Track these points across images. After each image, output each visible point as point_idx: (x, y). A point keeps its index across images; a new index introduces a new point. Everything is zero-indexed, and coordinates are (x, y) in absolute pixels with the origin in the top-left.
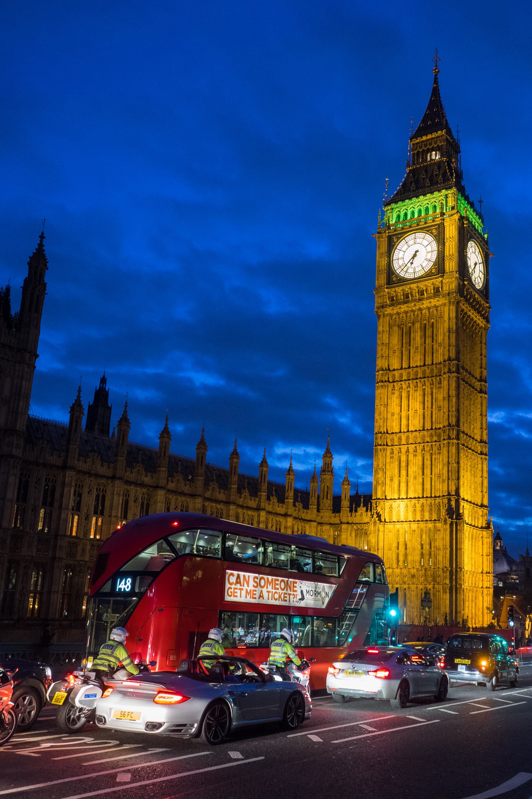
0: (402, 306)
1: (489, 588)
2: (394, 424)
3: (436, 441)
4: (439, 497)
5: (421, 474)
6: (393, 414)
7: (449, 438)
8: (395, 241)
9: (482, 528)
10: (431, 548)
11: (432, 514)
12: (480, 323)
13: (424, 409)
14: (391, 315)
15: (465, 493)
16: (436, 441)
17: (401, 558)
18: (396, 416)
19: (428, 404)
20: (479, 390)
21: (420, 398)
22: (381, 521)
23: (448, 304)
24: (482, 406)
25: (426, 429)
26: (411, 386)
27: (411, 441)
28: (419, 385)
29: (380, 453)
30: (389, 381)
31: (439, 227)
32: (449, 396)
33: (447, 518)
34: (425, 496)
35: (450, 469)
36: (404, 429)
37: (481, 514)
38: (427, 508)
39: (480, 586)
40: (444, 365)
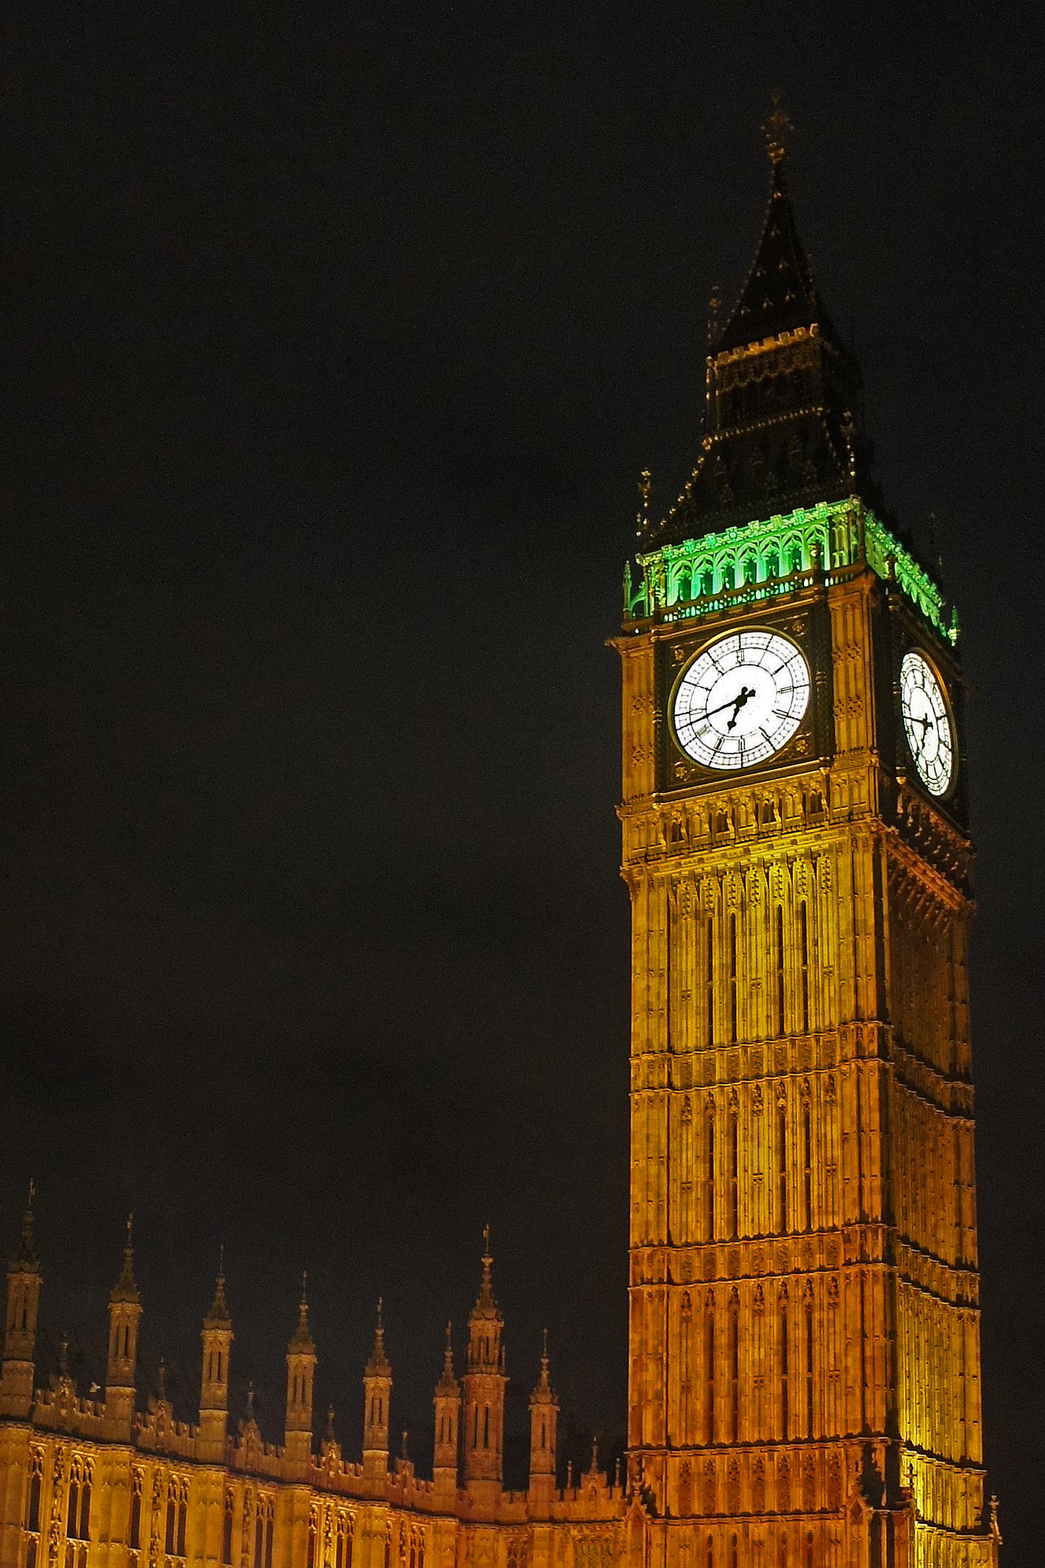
0: (705, 855)
2: (692, 1215)
4: (836, 1439)
5: (777, 1369)
6: (686, 1188)
7: (864, 1260)
13: (783, 1169)
14: (673, 883)
16: (822, 1269)
18: (697, 1193)
19: (796, 1155)
20: (947, 1105)
21: (769, 1137)
22: (656, 1516)
23: (847, 848)
24: (958, 1158)
25: (790, 1231)
26: (741, 1098)
27: (745, 1268)
28: (765, 1093)
29: (649, 1309)
30: (670, 1085)
32: (860, 1129)
34: (791, 1438)
35: (868, 1353)
36: (721, 1230)
38: (798, 1476)
40: (844, 1035)
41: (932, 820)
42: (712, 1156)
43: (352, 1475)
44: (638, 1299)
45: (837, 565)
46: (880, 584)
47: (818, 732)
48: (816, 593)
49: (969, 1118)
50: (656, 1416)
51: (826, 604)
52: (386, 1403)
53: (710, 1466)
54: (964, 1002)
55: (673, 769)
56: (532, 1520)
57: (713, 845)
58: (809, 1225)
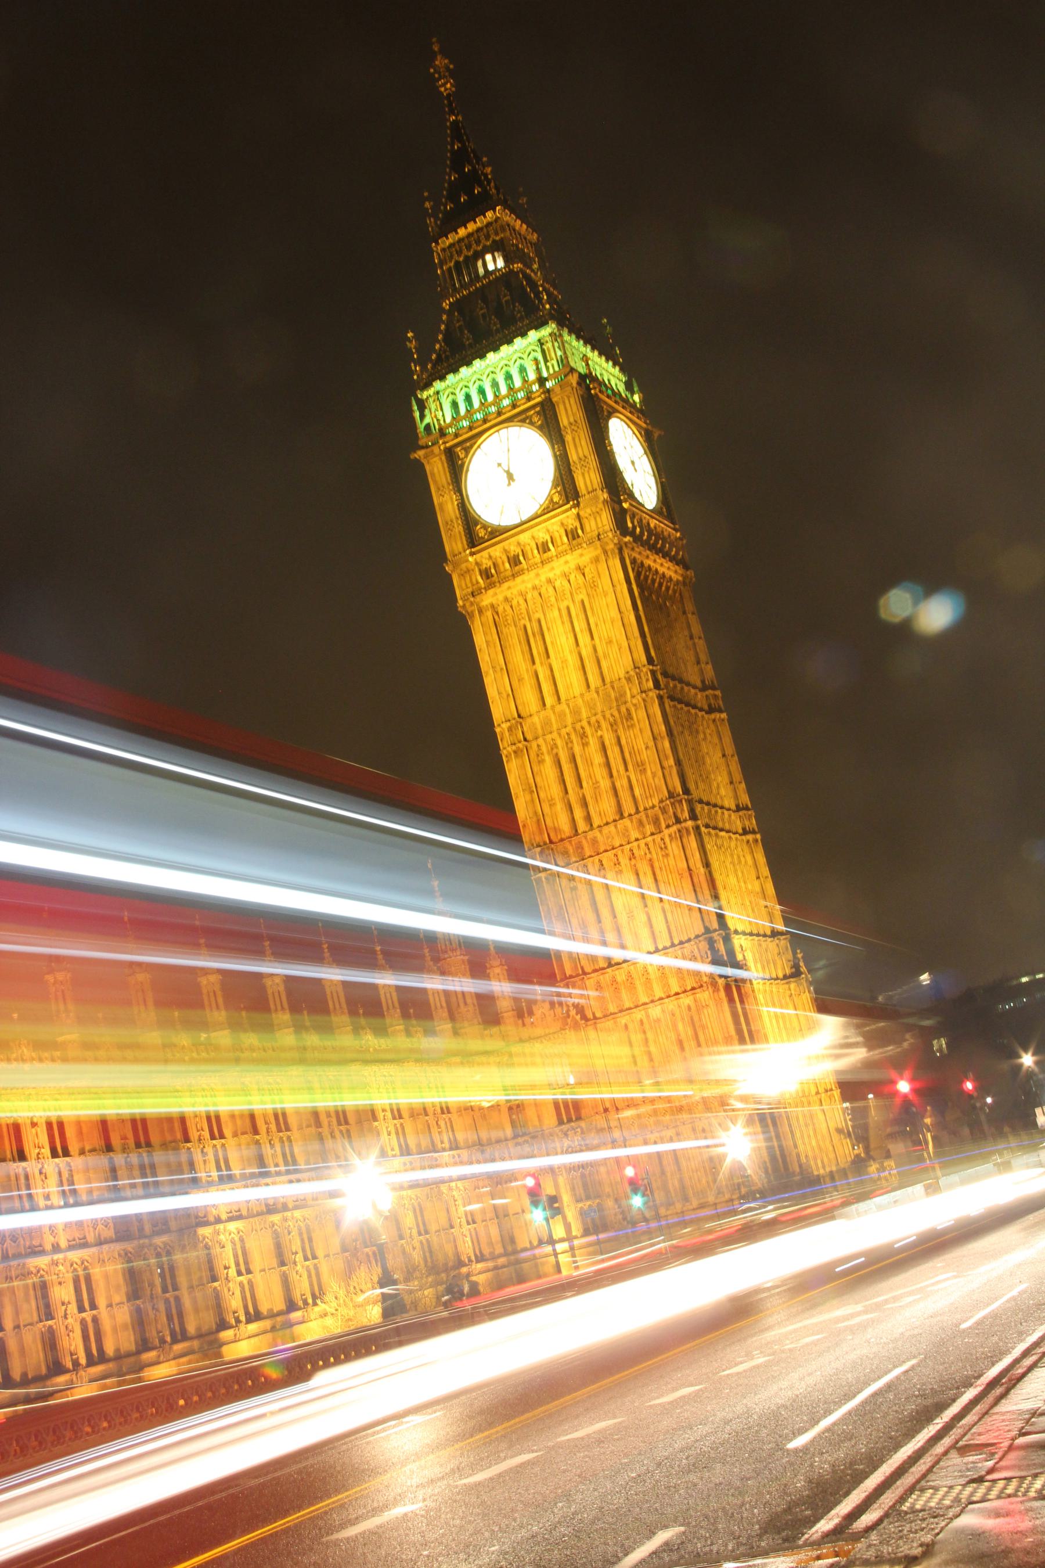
1: (831, 1090)
3: (652, 834)
4: (689, 940)
7: (678, 821)
9: (785, 977)
13: (611, 776)
15: (736, 919)
20: (706, 707)
21: (598, 759)
22: (586, 1019)
31: (543, 409)
34: (660, 947)
36: (582, 826)
37: (776, 951)
41: (652, 526)
45: (551, 371)
46: (582, 378)
47: (567, 487)
49: (720, 711)
51: (550, 400)
54: (700, 638)
57: (514, 576)
58: (637, 809)
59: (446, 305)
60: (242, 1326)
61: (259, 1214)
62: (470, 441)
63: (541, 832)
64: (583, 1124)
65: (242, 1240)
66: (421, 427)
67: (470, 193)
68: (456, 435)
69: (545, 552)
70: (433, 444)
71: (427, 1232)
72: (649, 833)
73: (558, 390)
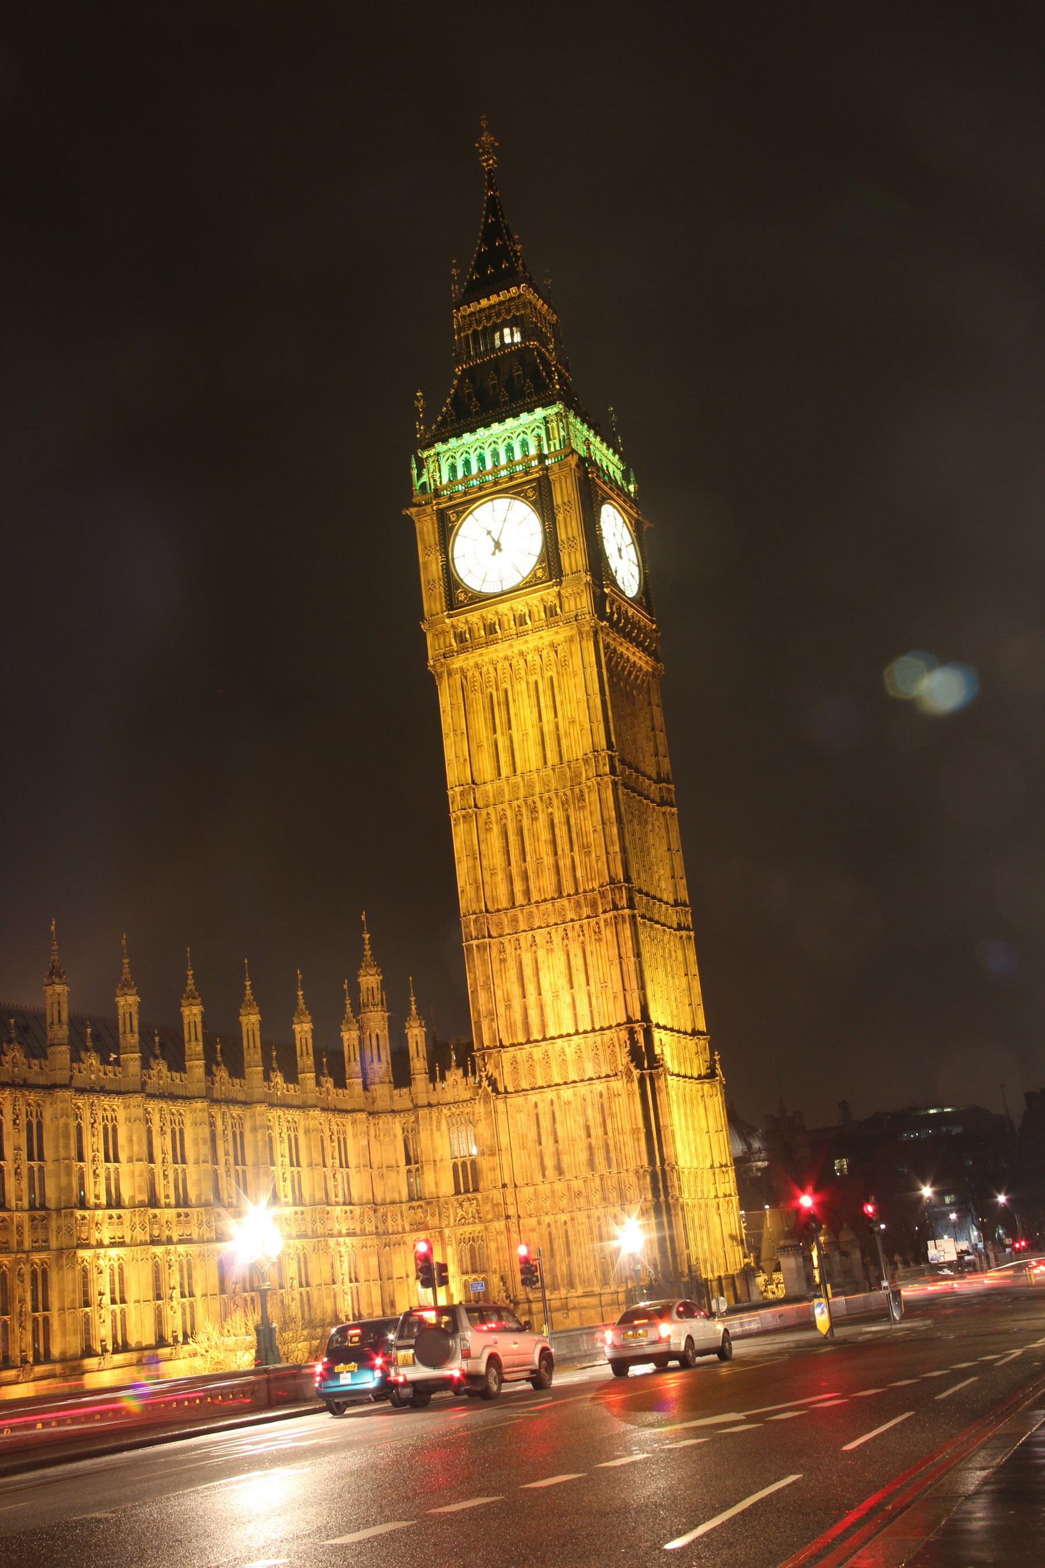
1: (730, 1195)
3: (588, 917)
4: (610, 1027)
5: (567, 986)
7: (615, 908)
8: (453, 519)
9: (700, 1077)
10: (606, 1133)
11: (599, 1065)
12: (644, 665)
17: (549, 1162)
20: (658, 799)
21: (545, 835)
22: (498, 1093)
33: (633, 1069)
34: (581, 1030)
36: (520, 899)
37: (694, 1050)
39: (712, 1195)
41: (630, 614)
42: (508, 851)
43: (292, 1092)
44: (470, 948)
45: (552, 450)
46: (582, 460)
48: (541, 469)
49: (672, 806)
50: (490, 1027)
51: (548, 477)
52: (310, 1041)
53: (531, 1056)
54: (661, 731)
55: (456, 595)
56: (416, 1107)
57: (488, 644)
58: (577, 890)
59: (458, 371)
60: (108, 1355)
61: (142, 1244)
62: (463, 505)
63: (478, 901)
64: (479, 1196)
65: (121, 1268)
66: (417, 485)
67: (497, 267)
68: (451, 498)
69: (521, 625)
70: (426, 504)
71: (308, 1285)
72: (585, 915)
73: (556, 468)
